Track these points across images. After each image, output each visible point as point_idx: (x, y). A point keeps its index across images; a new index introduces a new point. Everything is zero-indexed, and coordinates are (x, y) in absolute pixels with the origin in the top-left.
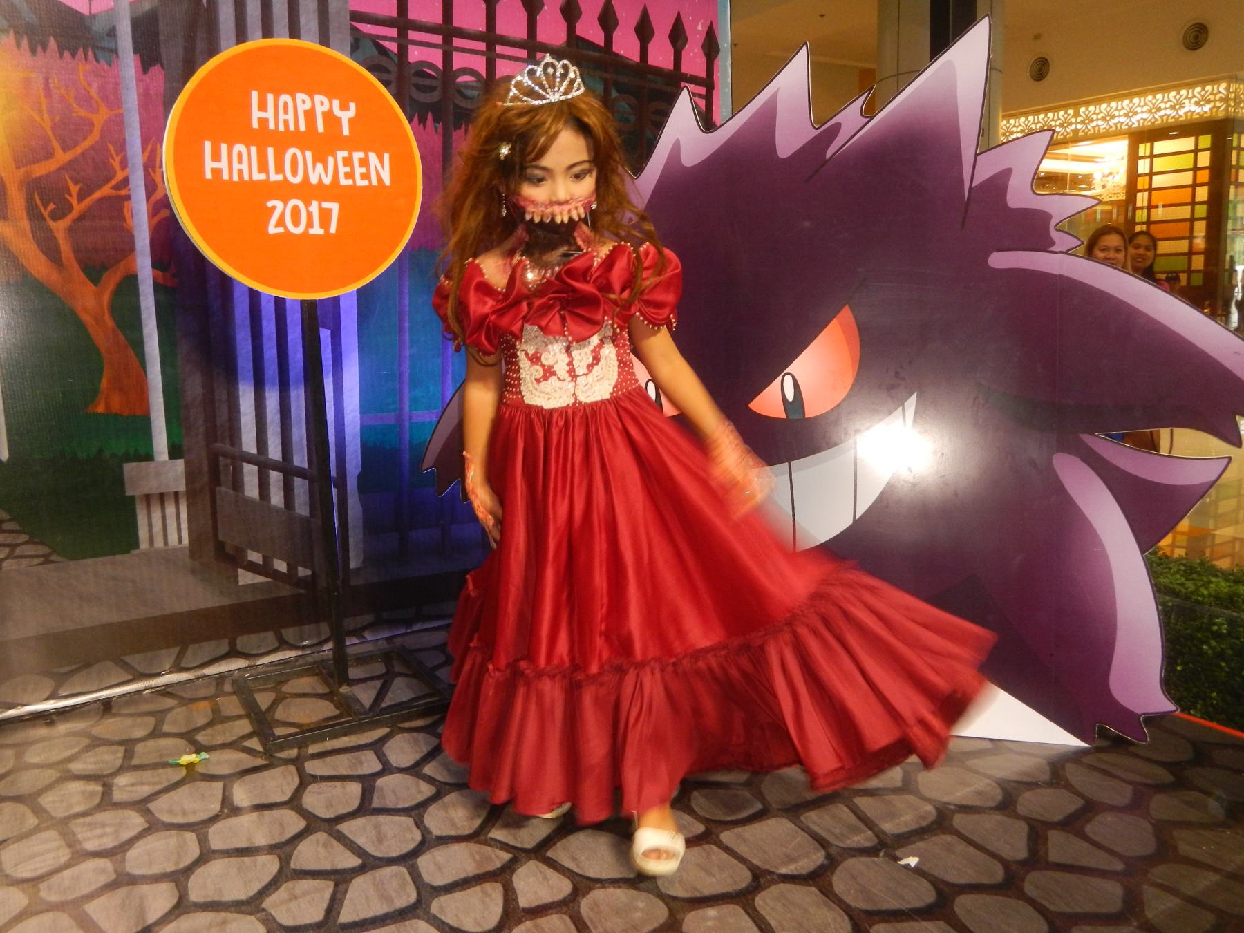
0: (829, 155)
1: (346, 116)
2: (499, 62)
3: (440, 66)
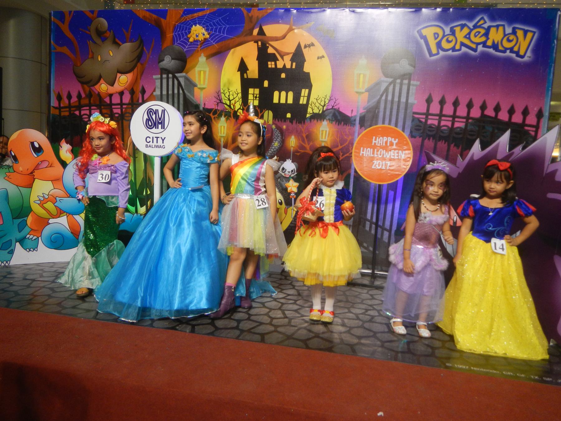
1: (395, 142)
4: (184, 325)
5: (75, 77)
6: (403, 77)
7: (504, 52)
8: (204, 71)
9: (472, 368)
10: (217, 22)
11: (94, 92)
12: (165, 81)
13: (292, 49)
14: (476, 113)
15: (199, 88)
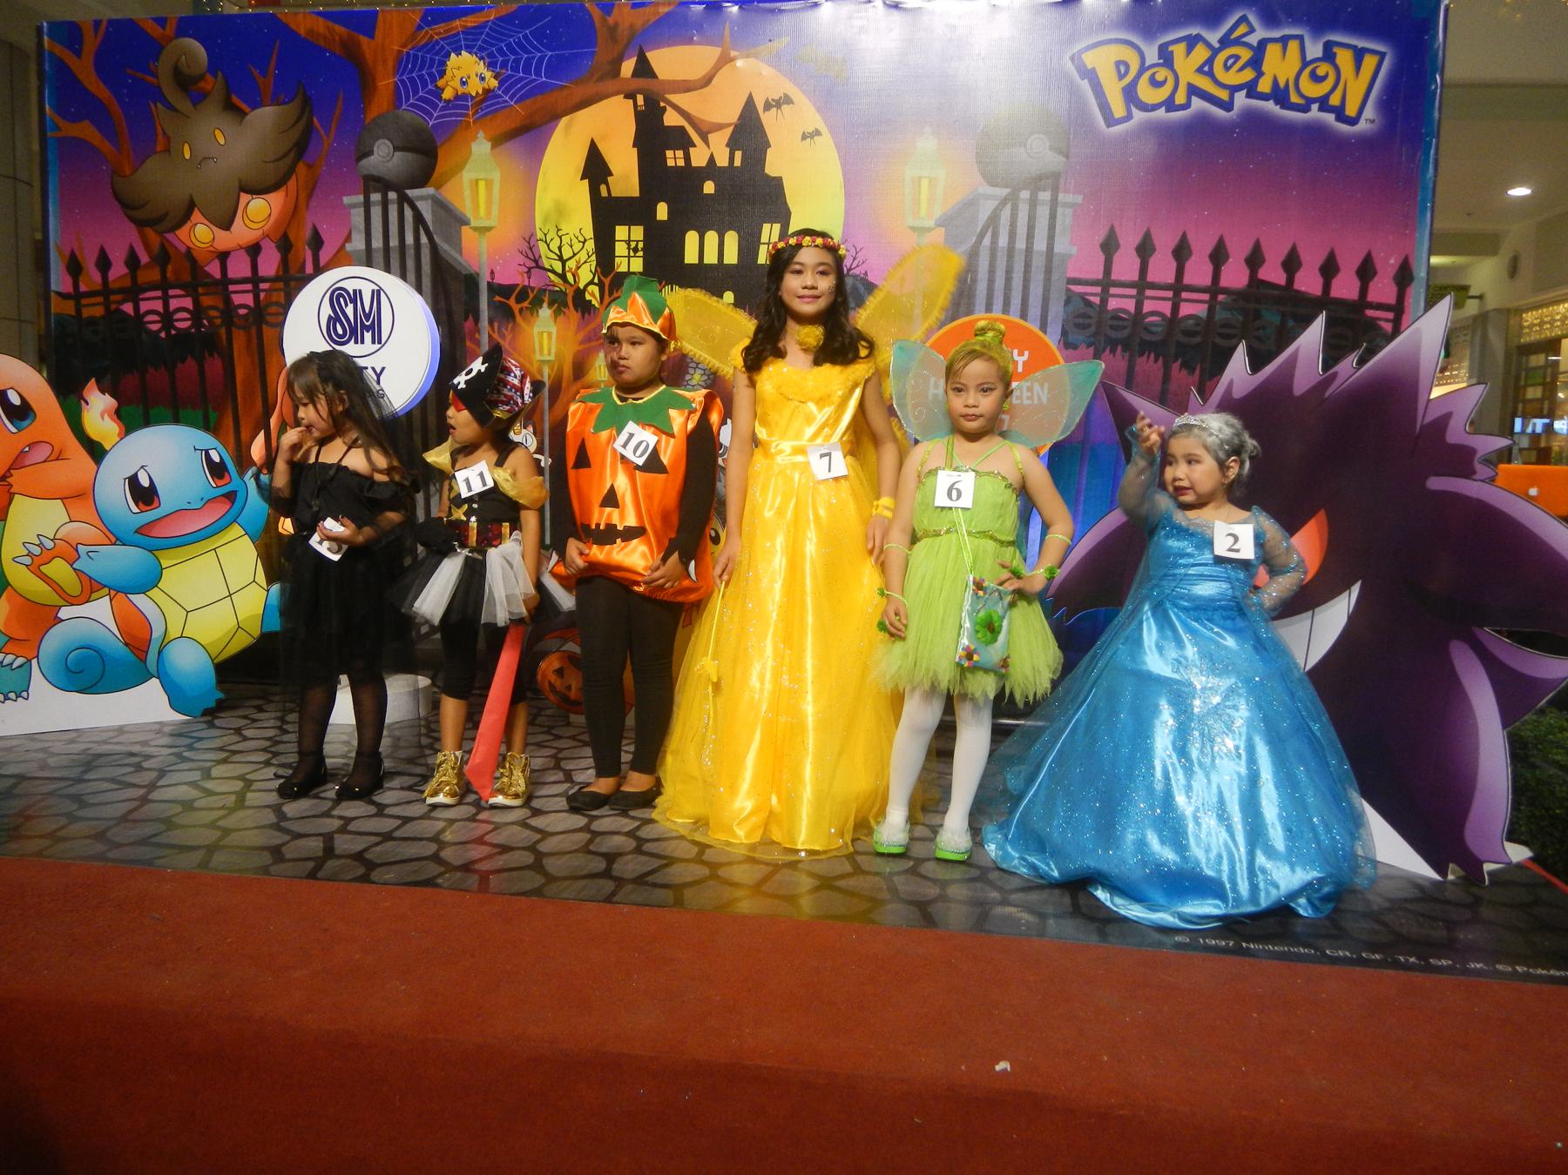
0: (1327, 394)
1: (1021, 360)
2: (1182, 304)
3: (1132, 309)
4: (459, 874)
5: (119, 206)
6: (1037, 182)
7: (1305, 108)
8: (486, 180)
9: (1244, 944)
10: (519, 44)
11: (176, 248)
12: (376, 212)
13: (732, 114)
14: (1235, 276)
15: (475, 229)
